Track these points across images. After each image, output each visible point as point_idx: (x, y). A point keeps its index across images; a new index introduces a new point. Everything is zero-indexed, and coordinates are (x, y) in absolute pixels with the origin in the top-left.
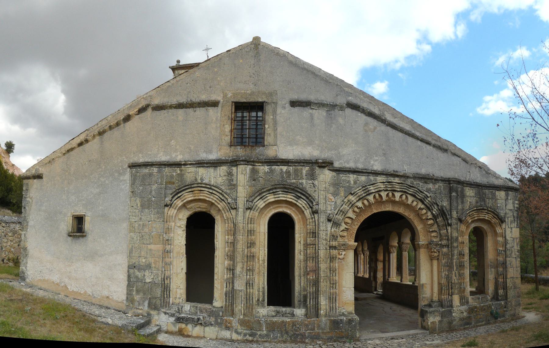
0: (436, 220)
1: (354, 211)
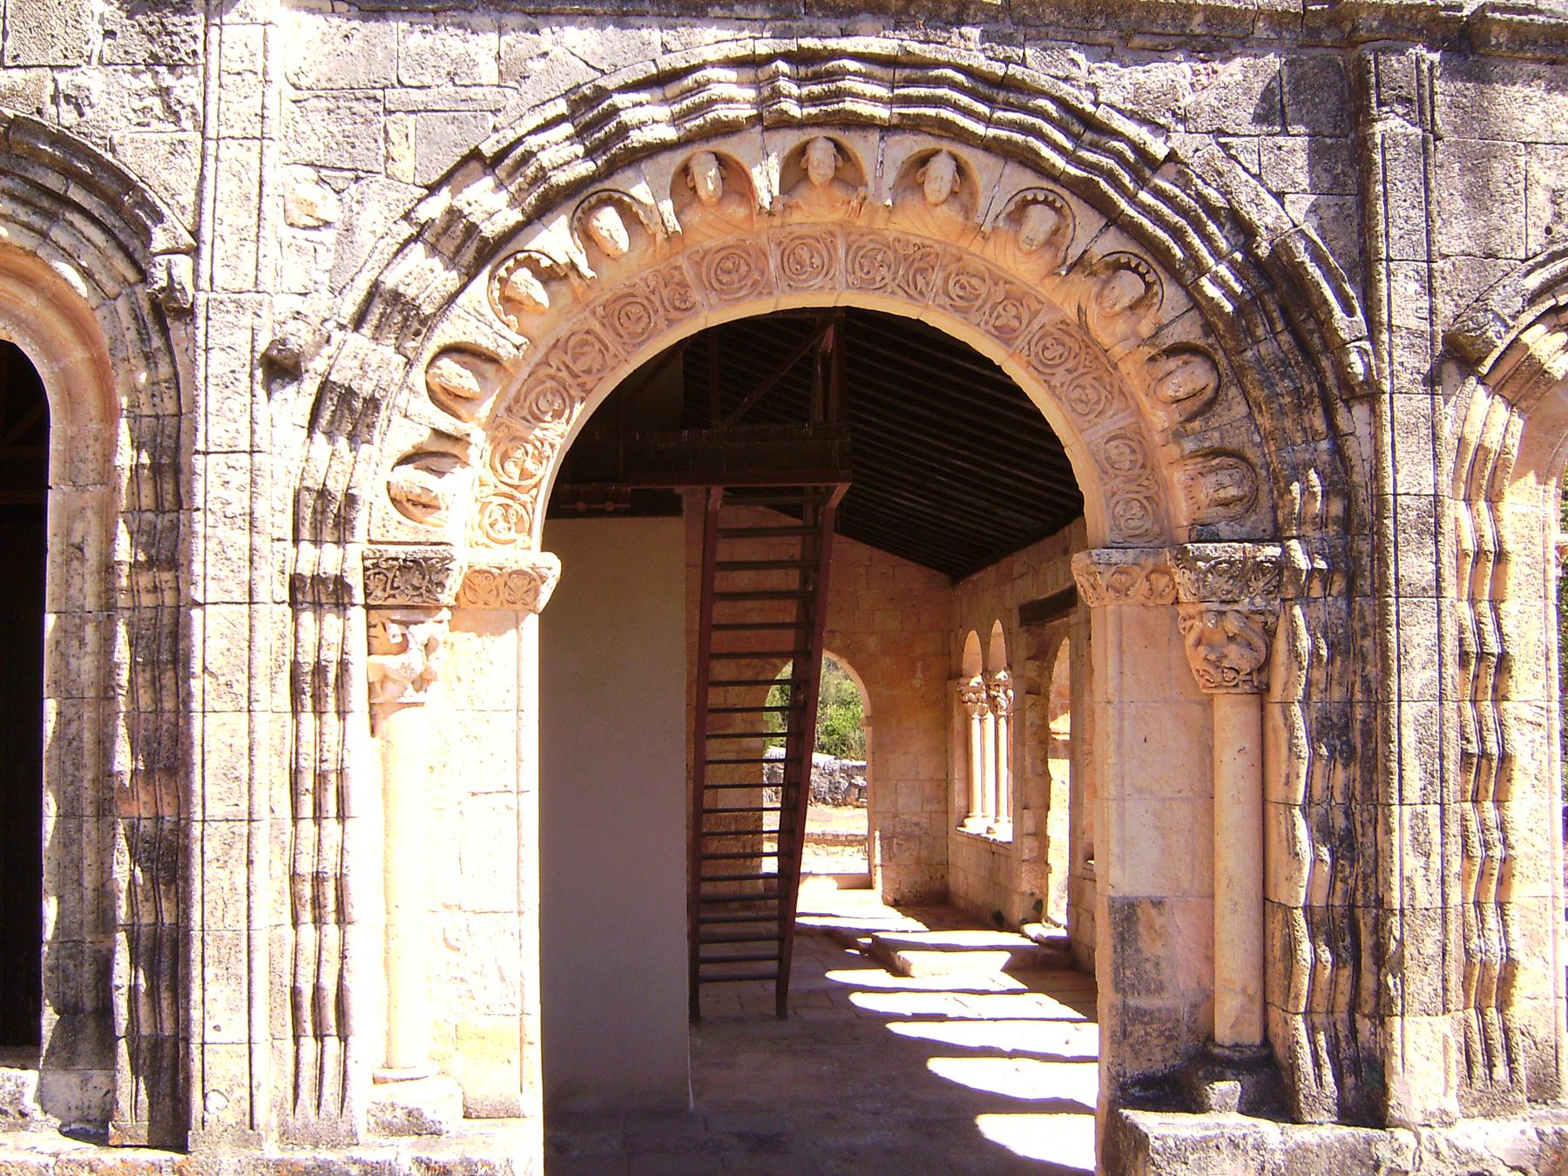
1: (510, 303)
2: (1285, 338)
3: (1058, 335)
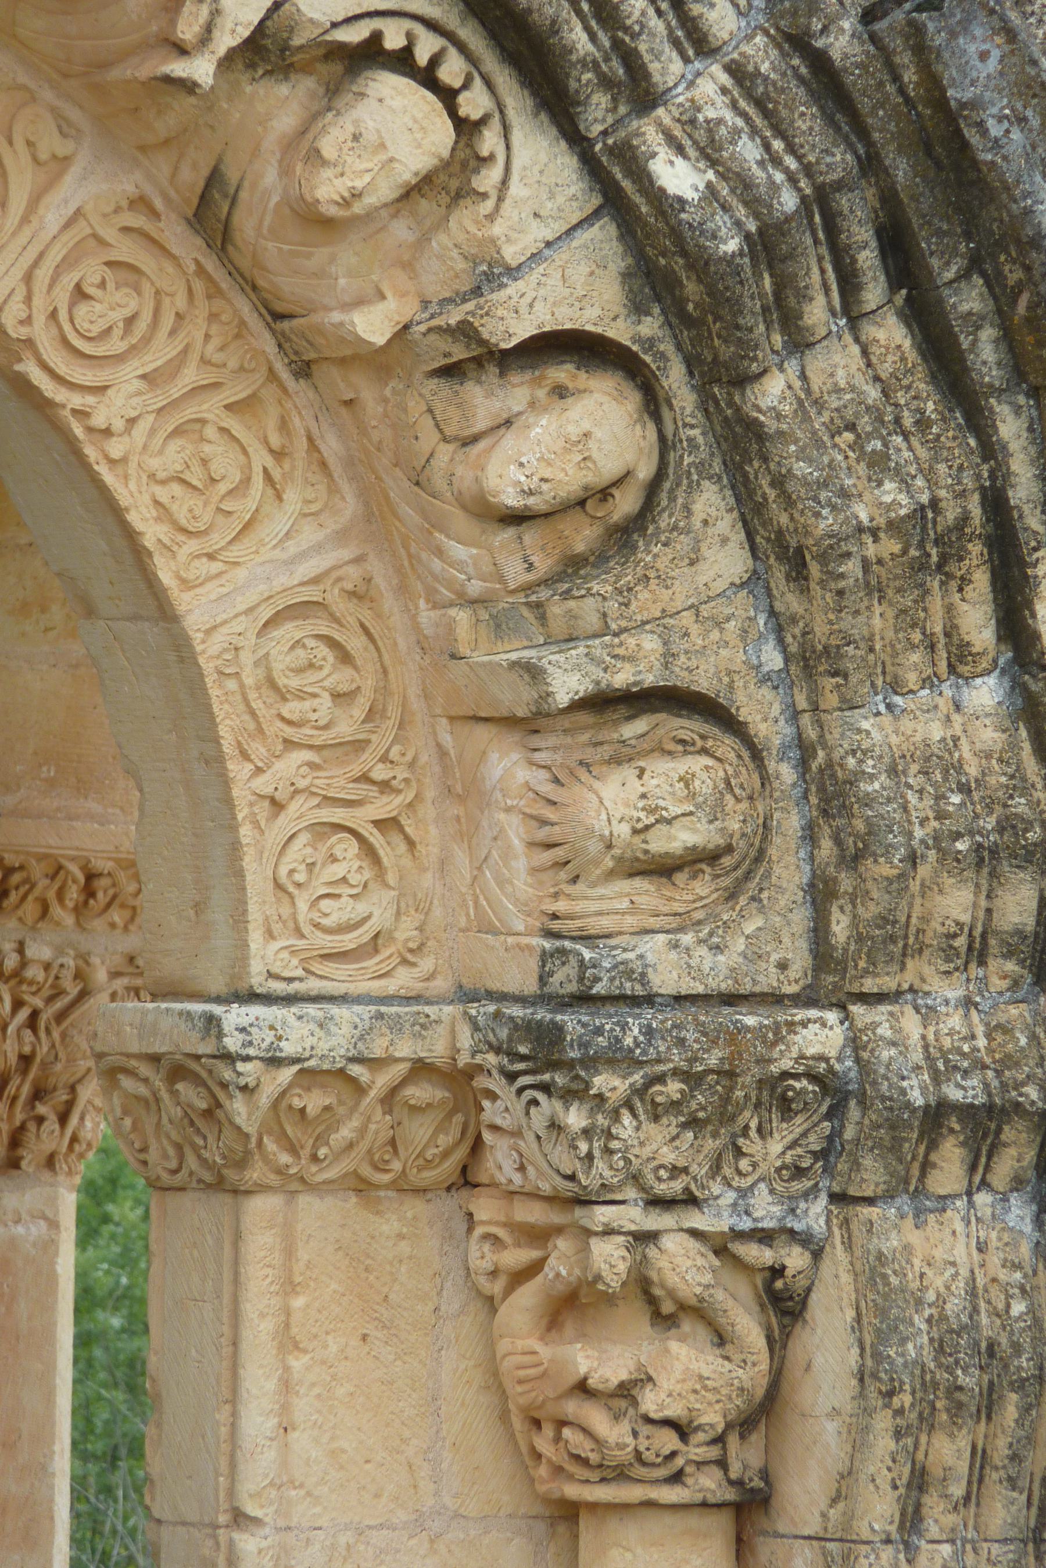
0: (722, 376)
2: (891, 334)
3: (126, 250)
